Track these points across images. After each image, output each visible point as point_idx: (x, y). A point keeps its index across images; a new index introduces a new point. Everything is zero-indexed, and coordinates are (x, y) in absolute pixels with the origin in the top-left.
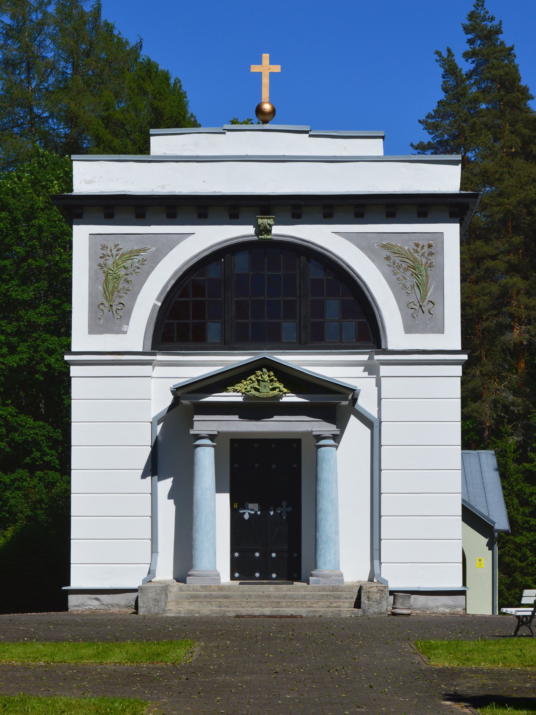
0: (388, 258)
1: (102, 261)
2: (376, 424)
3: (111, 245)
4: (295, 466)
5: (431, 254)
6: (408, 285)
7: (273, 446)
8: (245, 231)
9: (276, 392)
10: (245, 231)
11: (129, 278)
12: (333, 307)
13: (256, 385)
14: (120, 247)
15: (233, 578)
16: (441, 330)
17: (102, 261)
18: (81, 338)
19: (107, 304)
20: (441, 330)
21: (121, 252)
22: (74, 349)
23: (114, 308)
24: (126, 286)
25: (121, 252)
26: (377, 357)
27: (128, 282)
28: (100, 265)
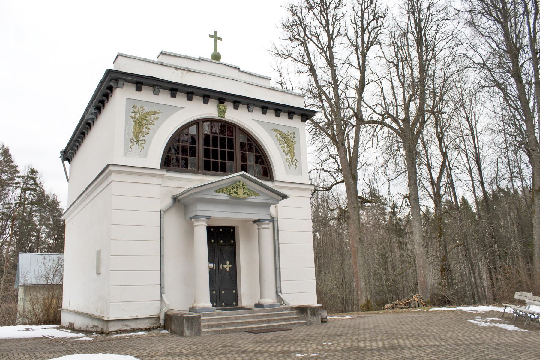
0: (277, 136)
1: (133, 115)
2: (276, 219)
4: (232, 241)
5: (294, 137)
6: (286, 150)
7: (221, 230)
8: (210, 110)
10: (210, 110)
11: (149, 126)
12: (251, 158)
13: (235, 190)
14: (144, 108)
17: (133, 115)
19: (135, 140)
21: (144, 111)
23: (140, 142)
24: (147, 131)
25: (144, 111)
27: (148, 128)
28: (132, 117)
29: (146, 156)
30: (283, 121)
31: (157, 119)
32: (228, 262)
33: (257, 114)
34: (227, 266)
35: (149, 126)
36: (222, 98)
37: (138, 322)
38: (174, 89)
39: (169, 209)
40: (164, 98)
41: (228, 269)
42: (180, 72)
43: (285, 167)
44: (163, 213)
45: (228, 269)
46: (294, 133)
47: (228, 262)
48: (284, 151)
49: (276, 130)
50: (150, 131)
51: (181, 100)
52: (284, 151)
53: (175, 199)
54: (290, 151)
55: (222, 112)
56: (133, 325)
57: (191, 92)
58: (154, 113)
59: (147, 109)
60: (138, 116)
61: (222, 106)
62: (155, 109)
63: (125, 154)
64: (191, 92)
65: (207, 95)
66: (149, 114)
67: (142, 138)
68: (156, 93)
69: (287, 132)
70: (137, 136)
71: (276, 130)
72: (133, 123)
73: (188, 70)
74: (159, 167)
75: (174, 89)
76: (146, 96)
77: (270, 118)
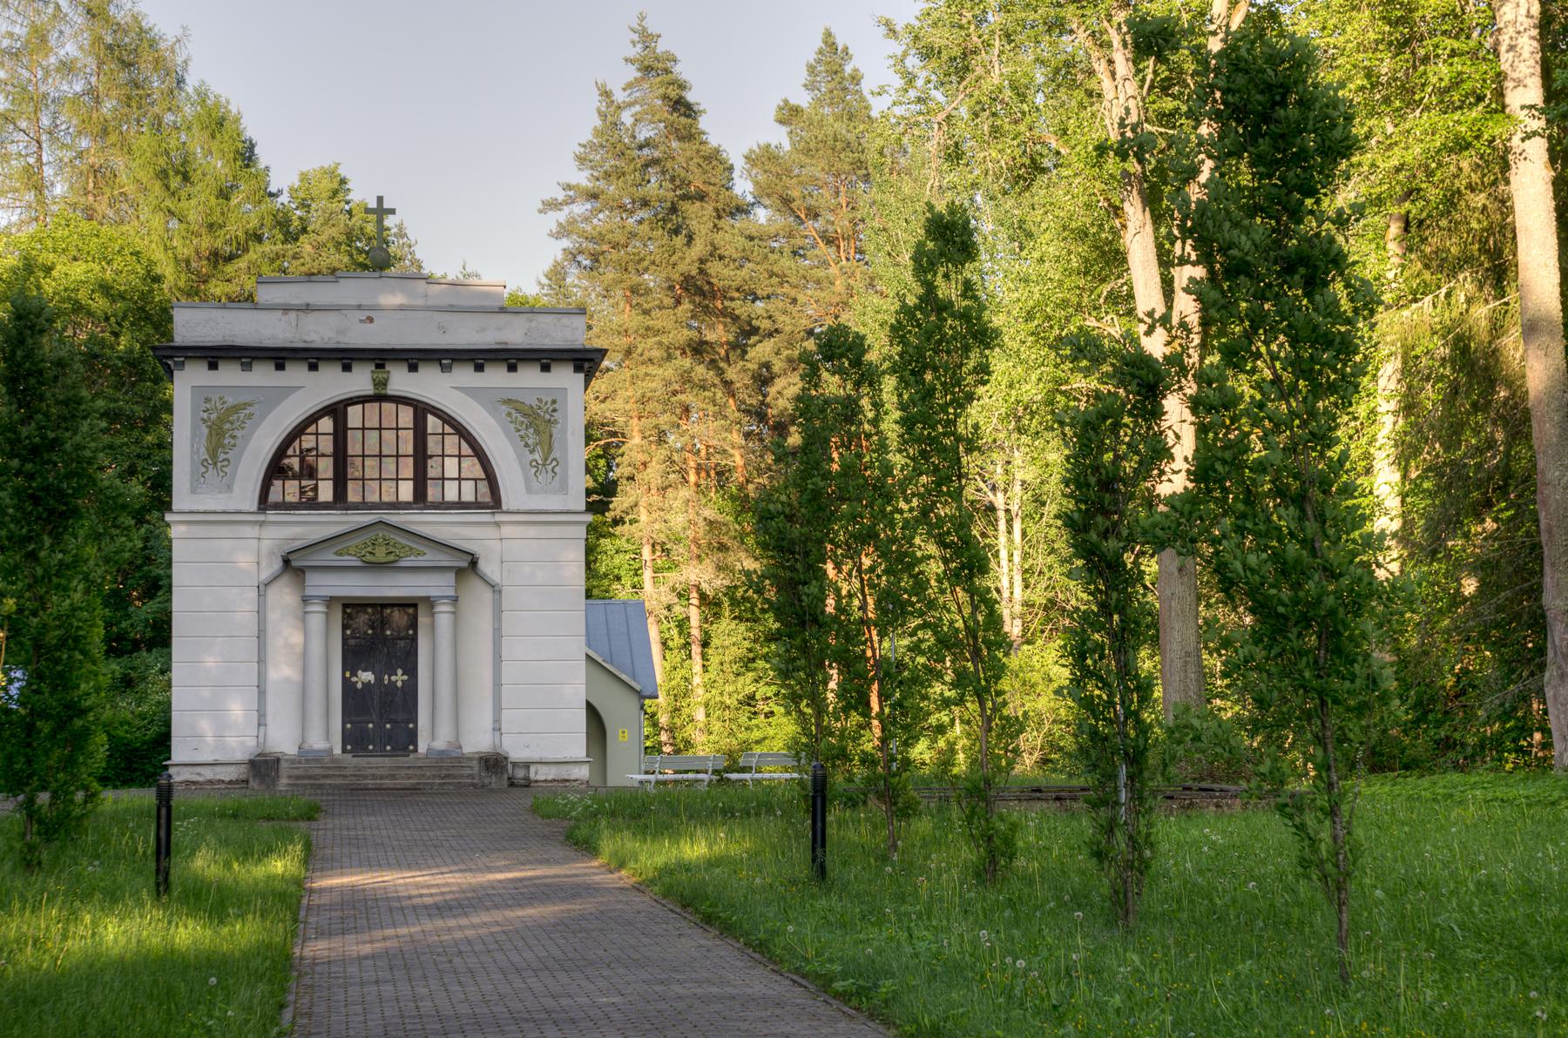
0: (509, 414)
1: (205, 416)
3: (215, 398)
6: (530, 442)
9: (392, 558)
11: (236, 433)
15: (344, 751)
16: (564, 489)
17: (205, 416)
18: (182, 496)
20: (564, 489)
22: (175, 507)
26: (499, 518)
27: (234, 437)
29: (229, 488)
30: (529, 378)
31: (250, 416)
32: (400, 672)
33: (464, 375)
34: (399, 678)
35: (236, 433)
36: (380, 358)
37: (218, 769)
38: (280, 357)
39: (275, 578)
40: (263, 376)
41: (399, 684)
42: (293, 315)
43: (527, 479)
44: (263, 588)
45: (399, 684)
46: (554, 402)
47: (400, 672)
48: (526, 445)
49: (508, 402)
50: (238, 442)
51: (296, 374)
52: (526, 445)
53: (286, 562)
54: (539, 443)
55: (381, 383)
56: (208, 774)
57: (314, 357)
58: (246, 405)
59: (231, 401)
60: (213, 416)
61: (381, 376)
62: (241, 400)
63: (193, 491)
64: (314, 357)
65: (346, 358)
66: (236, 409)
67: (223, 456)
68: (247, 367)
69: (535, 403)
70: (213, 454)
71: (508, 402)
72: (206, 431)
73: (307, 308)
74: (255, 508)
75: (280, 357)
76: (229, 376)
77: (496, 377)
